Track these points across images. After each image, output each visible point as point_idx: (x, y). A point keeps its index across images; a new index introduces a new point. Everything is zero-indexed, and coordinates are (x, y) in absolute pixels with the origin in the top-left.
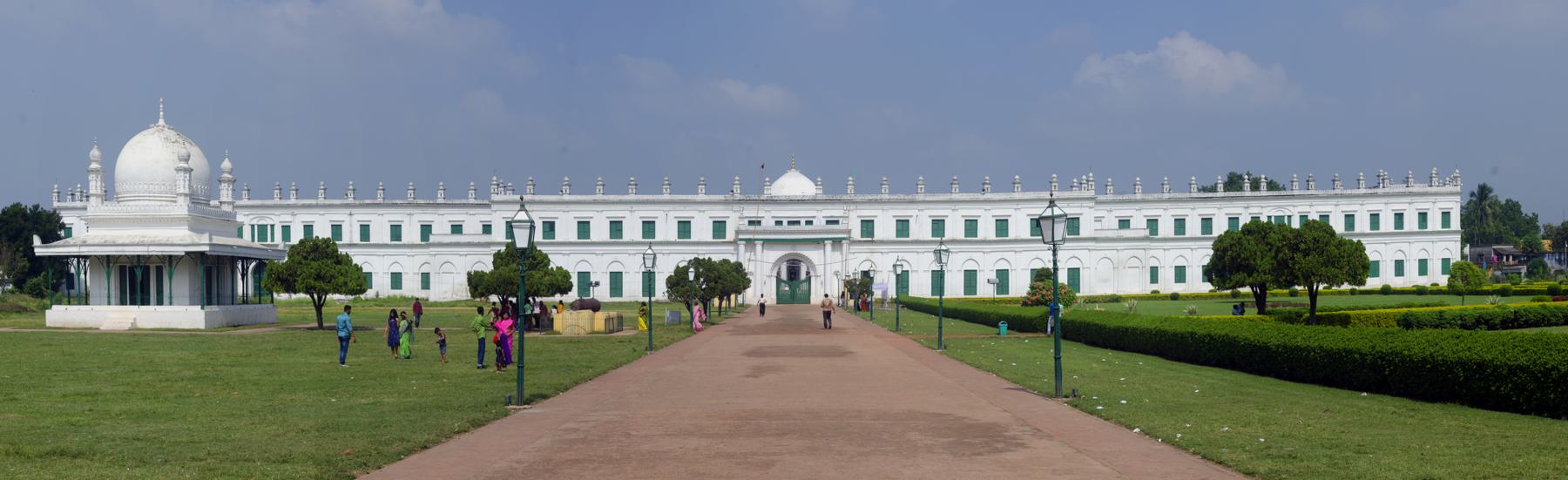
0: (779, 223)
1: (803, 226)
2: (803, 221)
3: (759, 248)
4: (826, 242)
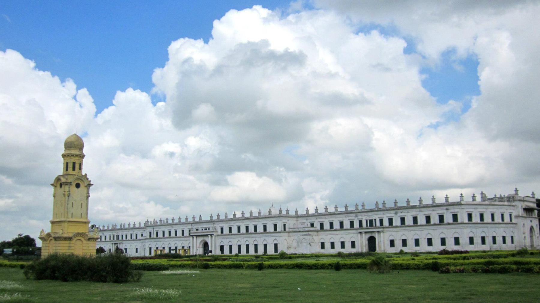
0: (202, 229)
1: (207, 230)
2: (207, 229)
3: (195, 238)
4: (209, 236)
